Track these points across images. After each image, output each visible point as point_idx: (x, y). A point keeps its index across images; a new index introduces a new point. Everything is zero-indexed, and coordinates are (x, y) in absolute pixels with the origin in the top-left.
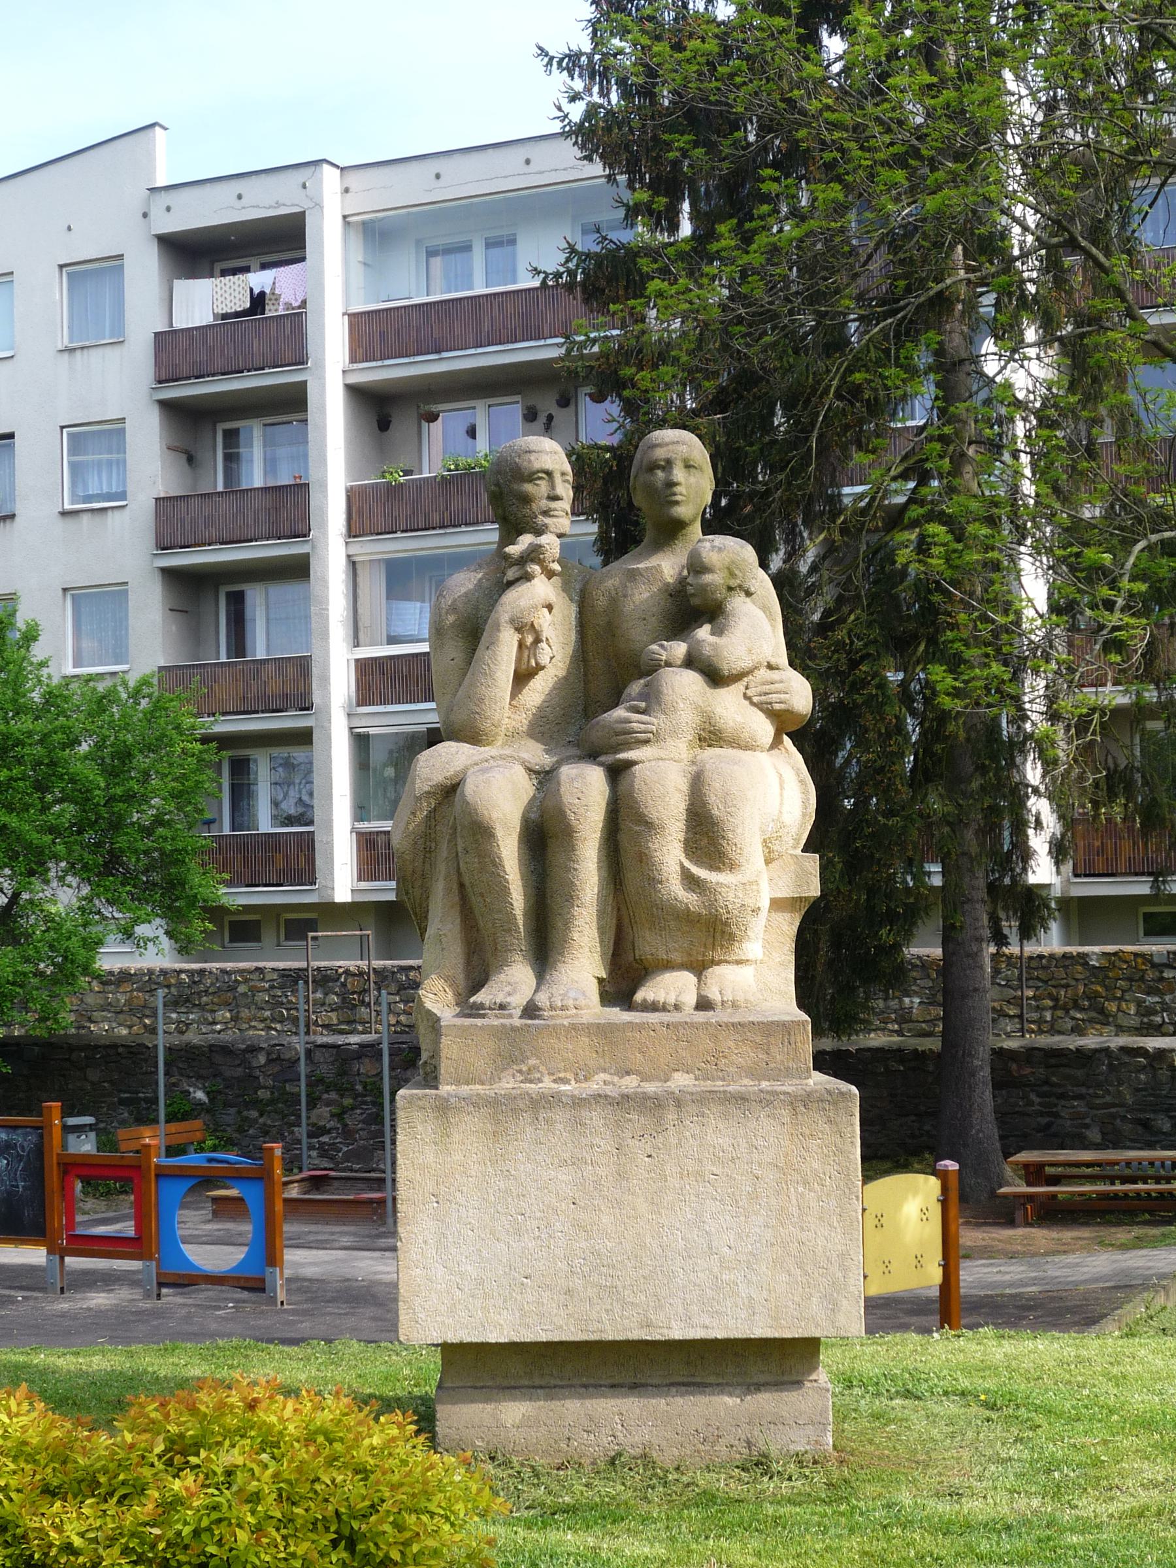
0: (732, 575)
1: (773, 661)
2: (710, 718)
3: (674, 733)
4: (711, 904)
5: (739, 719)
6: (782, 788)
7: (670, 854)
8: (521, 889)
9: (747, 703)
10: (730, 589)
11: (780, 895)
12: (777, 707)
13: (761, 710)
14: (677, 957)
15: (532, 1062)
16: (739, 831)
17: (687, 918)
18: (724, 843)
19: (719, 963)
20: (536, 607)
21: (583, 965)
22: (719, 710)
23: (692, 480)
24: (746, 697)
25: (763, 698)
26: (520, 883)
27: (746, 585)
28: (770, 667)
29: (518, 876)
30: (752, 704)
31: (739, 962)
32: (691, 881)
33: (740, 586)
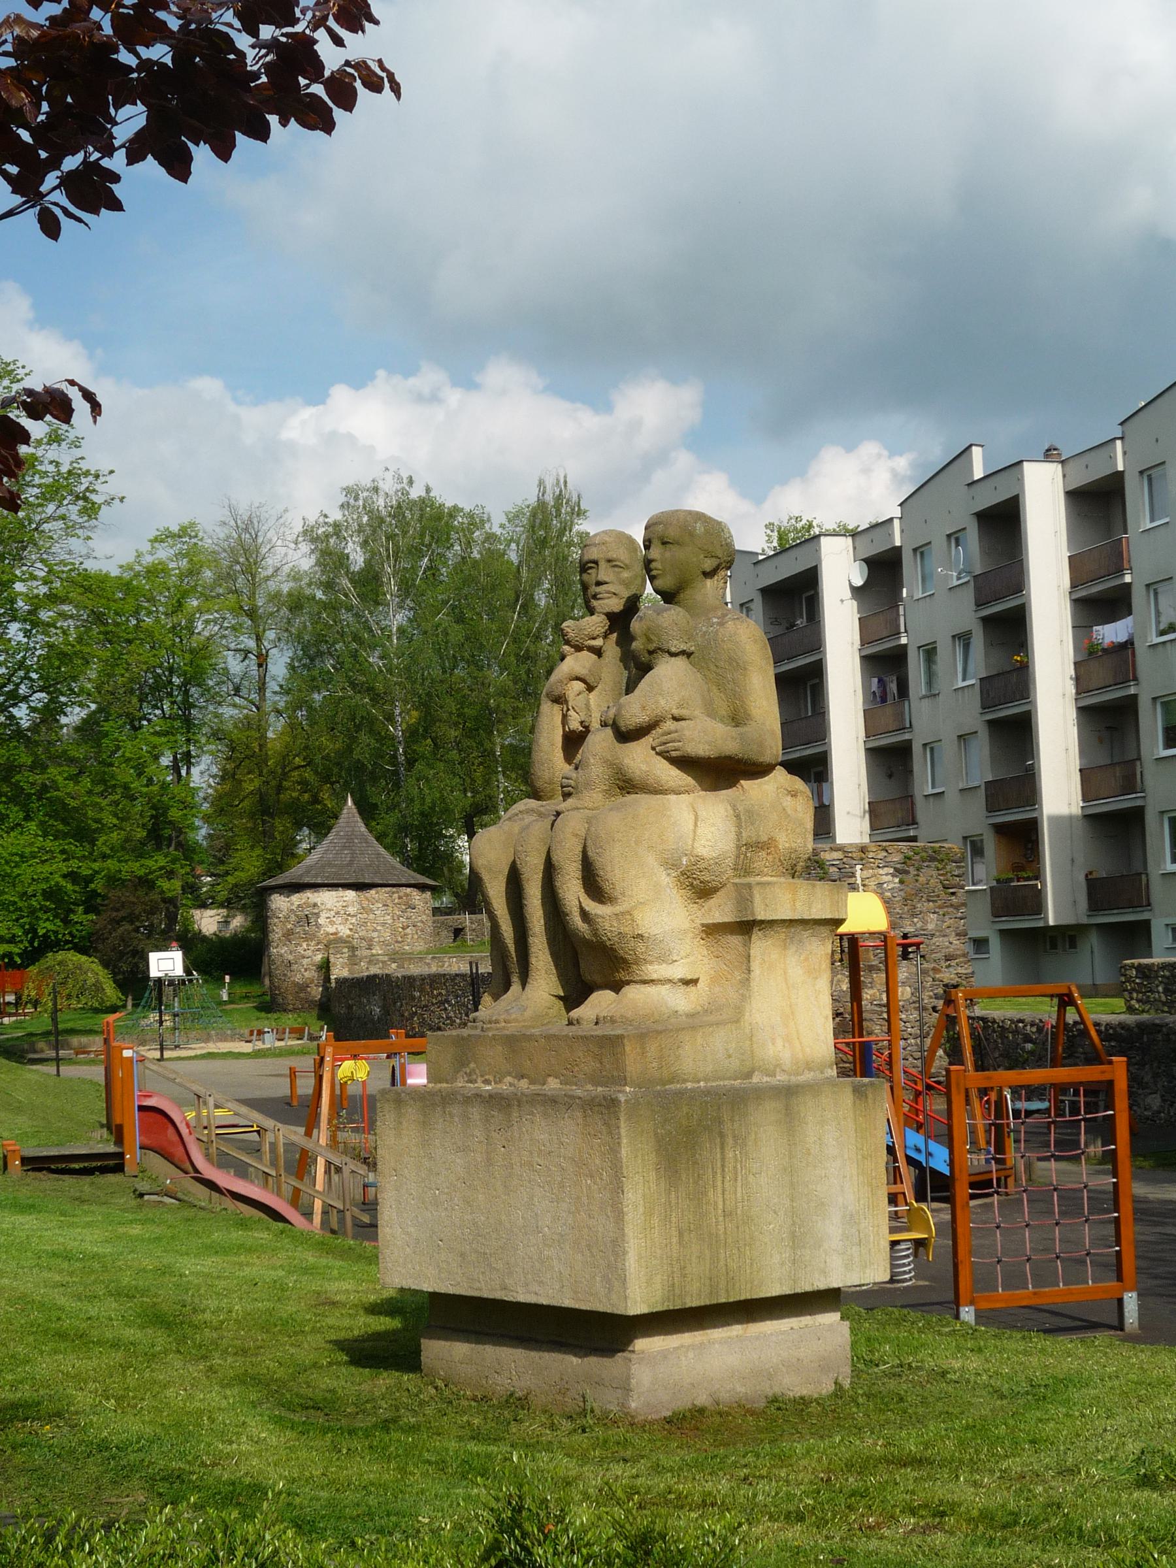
0: (649, 640)
1: (676, 712)
3: (588, 785)
4: (595, 932)
5: (644, 767)
6: (696, 825)
7: (572, 892)
8: (509, 922)
10: (651, 653)
11: (726, 920)
12: (674, 754)
13: (666, 758)
14: (597, 978)
15: (472, 1065)
17: (587, 943)
18: (599, 879)
19: (628, 983)
20: (561, 682)
21: (544, 984)
23: (668, 555)
26: (508, 917)
27: (665, 647)
29: (506, 911)
30: (657, 754)
31: (645, 982)
32: (585, 915)
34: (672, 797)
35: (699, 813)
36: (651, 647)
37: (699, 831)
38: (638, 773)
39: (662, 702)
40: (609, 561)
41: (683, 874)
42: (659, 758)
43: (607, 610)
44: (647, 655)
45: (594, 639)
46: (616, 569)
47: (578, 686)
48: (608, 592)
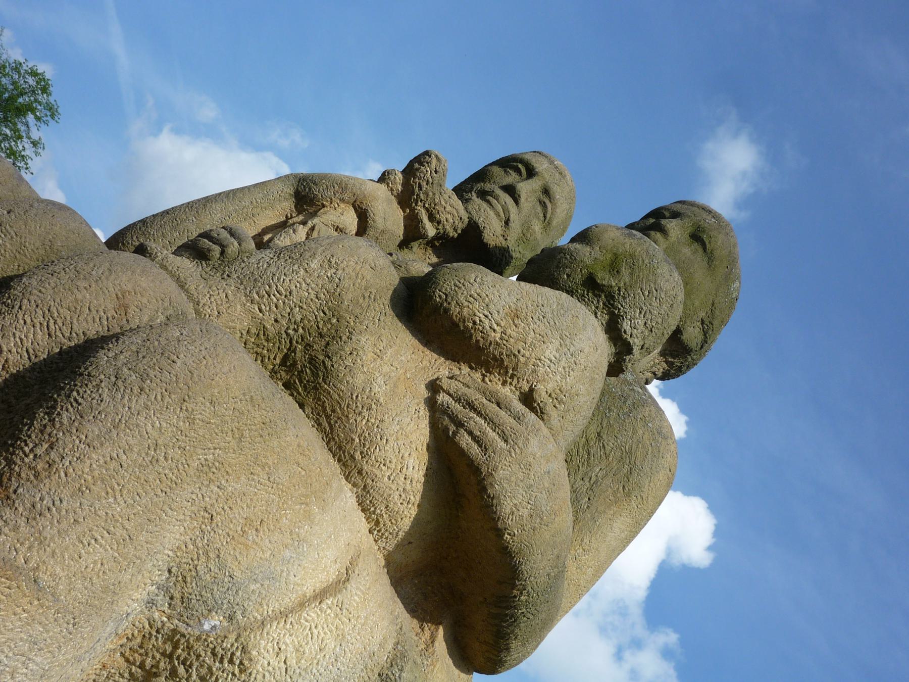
0: (614, 267)
1: (541, 395)
2: (336, 337)
5: (380, 389)
6: (320, 596)
9: (425, 393)
12: (465, 440)
13: (434, 425)
16: (92, 430)
22: (365, 342)
24: (434, 387)
25: (457, 408)
27: (623, 306)
28: (528, 399)
30: (431, 403)
33: (610, 297)
34: (348, 497)
35: (352, 586)
36: (604, 278)
37: (312, 614)
38: (359, 380)
39: (550, 351)
40: (546, 191)
41: (174, 638)
42: (424, 413)
43: (480, 222)
44: (578, 278)
45: (432, 218)
46: (539, 209)
47: (350, 220)
48: (506, 210)
